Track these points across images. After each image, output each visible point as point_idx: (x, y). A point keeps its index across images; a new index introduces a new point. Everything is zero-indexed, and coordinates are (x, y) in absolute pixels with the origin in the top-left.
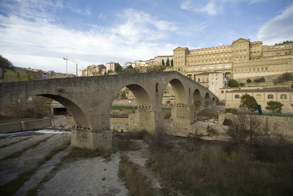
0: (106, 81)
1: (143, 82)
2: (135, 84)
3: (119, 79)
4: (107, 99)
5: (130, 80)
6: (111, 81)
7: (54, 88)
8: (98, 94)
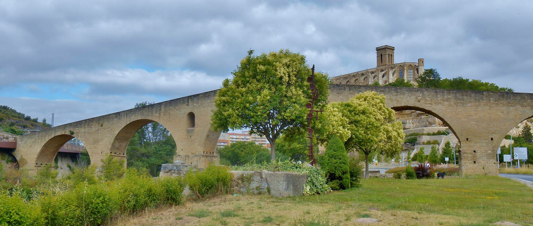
0: (107, 120)
1: (158, 115)
2: (143, 118)
3: (122, 116)
4: (107, 138)
5: (136, 115)
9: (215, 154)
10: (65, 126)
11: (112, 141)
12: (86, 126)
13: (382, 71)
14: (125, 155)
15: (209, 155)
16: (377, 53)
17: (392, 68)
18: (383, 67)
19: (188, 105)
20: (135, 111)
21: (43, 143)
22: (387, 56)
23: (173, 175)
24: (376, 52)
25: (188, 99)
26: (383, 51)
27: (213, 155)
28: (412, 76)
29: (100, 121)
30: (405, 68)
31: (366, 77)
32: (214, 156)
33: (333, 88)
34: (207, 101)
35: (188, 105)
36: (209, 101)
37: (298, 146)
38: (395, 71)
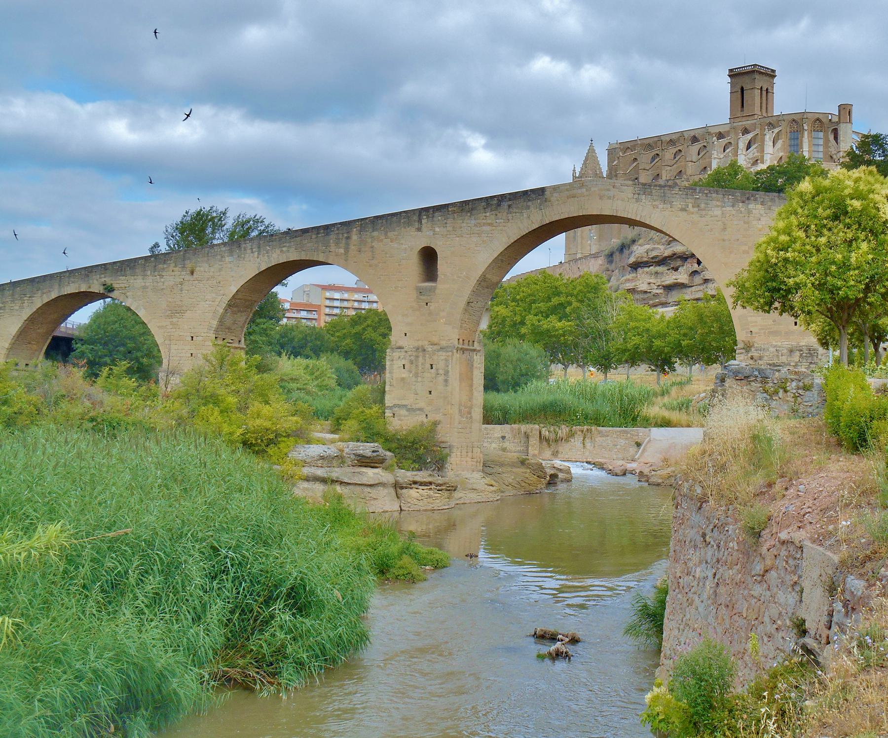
0: (206, 259)
1: (342, 251)
2: (304, 258)
3: (245, 250)
4: (207, 303)
5: (284, 249)
6: (219, 257)
7: (97, 280)
8: (181, 291)
9: (477, 346)
10: (89, 271)
11: (221, 311)
12: (149, 273)
13: (746, 131)
14: (243, 345)
15: (466, 347)
16: (731, 83)
17: (771, 126)
18: (748, 123)
19: (419, 229)
20: (280, 239)
21: (27, 313)
22: (757, 92)
23: (753, 384)
24: (729, 80)
25: (420, 215)
26: (746, 79)
27: (472, 348)
28: (821, 149)
29: (187, 262)
30: (806, 128)
31: (705, 146)
32: (474, 350)
33: (770, 203)
34: (469, 221)
35: (419, 229)
36: (473, 222)
37: (559, 325)
38: (778, 133)
